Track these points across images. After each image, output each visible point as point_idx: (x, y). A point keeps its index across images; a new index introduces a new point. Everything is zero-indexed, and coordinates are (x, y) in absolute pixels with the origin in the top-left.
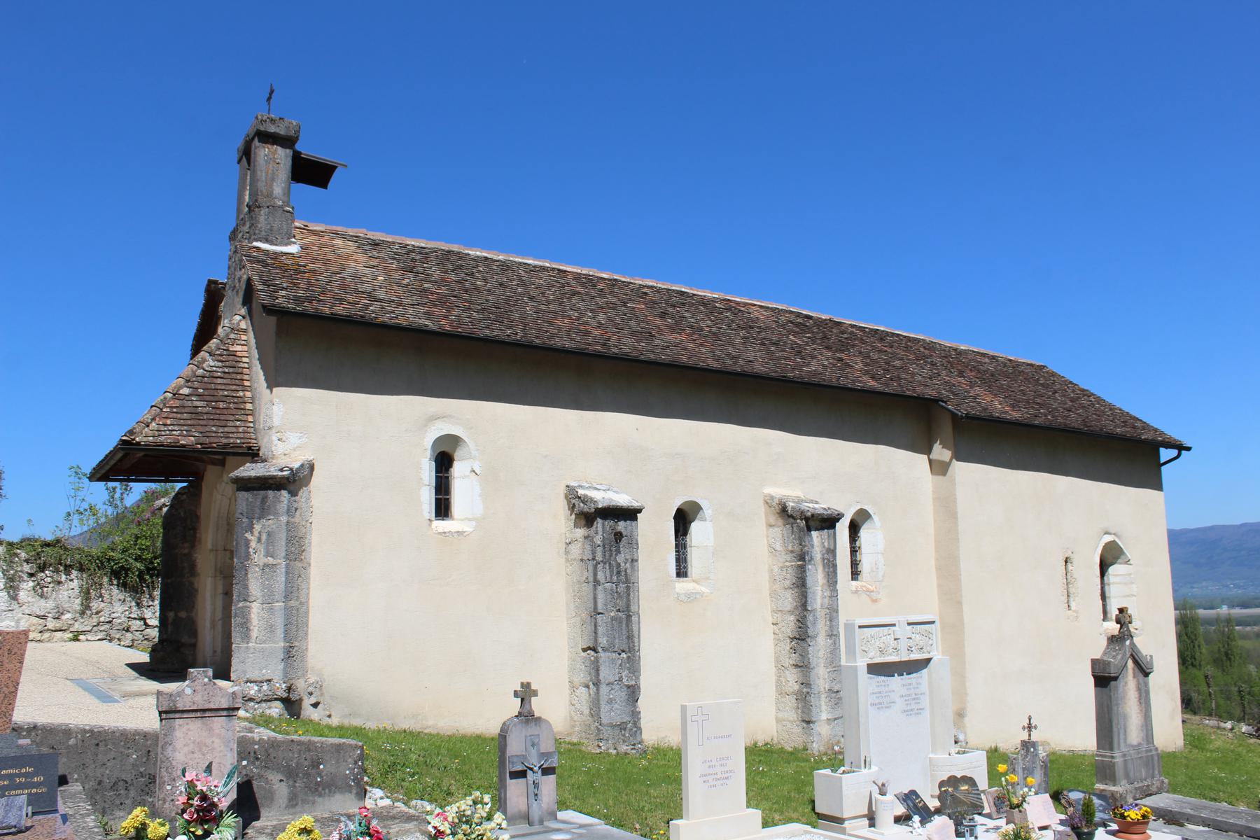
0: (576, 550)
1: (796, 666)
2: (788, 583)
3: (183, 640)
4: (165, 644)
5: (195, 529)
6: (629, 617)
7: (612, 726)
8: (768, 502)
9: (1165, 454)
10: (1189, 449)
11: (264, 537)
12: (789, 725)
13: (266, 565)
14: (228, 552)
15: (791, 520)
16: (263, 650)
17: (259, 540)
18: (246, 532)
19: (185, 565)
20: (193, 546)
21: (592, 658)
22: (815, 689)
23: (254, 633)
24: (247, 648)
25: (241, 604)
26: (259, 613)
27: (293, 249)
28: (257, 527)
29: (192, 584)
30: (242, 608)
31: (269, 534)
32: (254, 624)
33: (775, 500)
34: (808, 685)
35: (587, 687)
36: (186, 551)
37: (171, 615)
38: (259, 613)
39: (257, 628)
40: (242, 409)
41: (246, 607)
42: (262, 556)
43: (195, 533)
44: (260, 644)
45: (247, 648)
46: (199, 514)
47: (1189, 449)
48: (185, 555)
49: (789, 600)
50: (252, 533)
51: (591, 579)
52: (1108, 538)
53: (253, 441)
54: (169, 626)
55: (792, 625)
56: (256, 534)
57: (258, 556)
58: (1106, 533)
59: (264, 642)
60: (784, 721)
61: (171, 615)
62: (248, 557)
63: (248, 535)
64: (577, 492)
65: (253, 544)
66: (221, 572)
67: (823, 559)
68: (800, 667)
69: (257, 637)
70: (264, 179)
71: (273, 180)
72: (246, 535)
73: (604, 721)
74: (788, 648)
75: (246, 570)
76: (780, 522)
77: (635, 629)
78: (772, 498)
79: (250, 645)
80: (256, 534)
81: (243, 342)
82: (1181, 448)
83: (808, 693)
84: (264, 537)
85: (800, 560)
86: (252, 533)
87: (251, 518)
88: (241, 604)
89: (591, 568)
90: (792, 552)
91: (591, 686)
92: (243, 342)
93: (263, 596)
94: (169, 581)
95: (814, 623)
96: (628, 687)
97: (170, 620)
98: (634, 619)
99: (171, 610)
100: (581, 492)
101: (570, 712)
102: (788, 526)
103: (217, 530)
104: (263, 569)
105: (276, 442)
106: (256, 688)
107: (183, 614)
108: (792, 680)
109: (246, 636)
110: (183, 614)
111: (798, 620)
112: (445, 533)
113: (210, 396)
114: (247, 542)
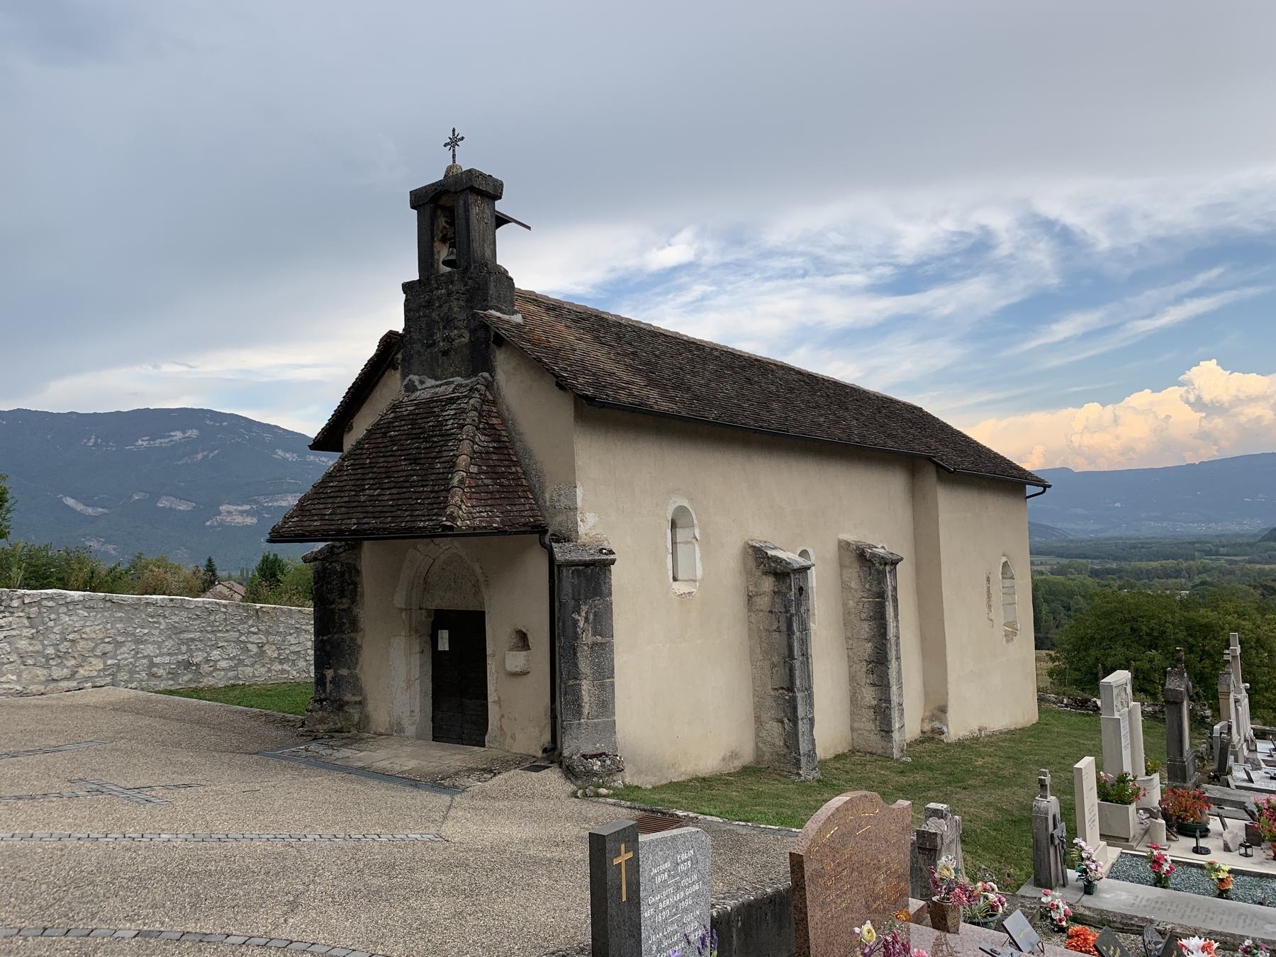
0: (763, 602)
1: (873, 685)
2: (864, 616)
3: (346, 698)
4: (324, 703)
5: (355, 584)
6: (808, 658)
7: (805, 755)
8: (844, 546)
9: (1030, 490)
10: (1050, 486)
11: (591, 617)
12: (866, 733)
13: (595, 644)
14: (423, 611)
15: (870, 563)
16: (596, 725)
17: (587, 620)
18: (573, 612)
19: (345, 621)
20: (353, 601)
21: (787, 698)
22: (892, 706)
23: (586, 711)
24: (579, 724)
25: (571, 683)
26: (590, 690)
27: (518, 318)
28: (584, 608)
29: (353, 640)
30: (572, 686)
31: (595, 615)
32: (585, 701)
33: (851, 546)
34: (888, 701)
35: (782, 722)
36: (345, 606)
37: (329, 674)
38: (590, 690)
39: (588, 704)
40: (520, 485)
41: (576, 684)
42: (590, 634)
43: (356, 587)
44: (592, 719)
45: (579, 724)
46: (359, 569)
47: (1050, 486)
48: (343, 610)
49: (866, 628)
50: (579, 614)
51: (784, 628)
52: (1004, 559)
53: (540, 518)
54: (328, 684)
55: (869, 651)
56: (583, 614)
57: (587, 635)
58: (1004, 555)
59: (597, 717)
60: (861, 730)
61: (329, 674)
62: (576, 636)
63: (577, 617)
64: (767, 554)
65: (581, 624)
66: (417, 631)
67: (892, 596)
68: (878, 686)
69: (589, 713)
70: (477, 240)
71: (484, 241)
72: (573, 616)
73: (802, 752)
74: (864, 669)
75: (574, 649)
76: (856, 565)
77: (811, 668)
78: (848, 544)
79: (582, 721)
80: (583, 614)
81: (496, 414)
82: (1046, 487)
83: (888, 707)
84: (591, 617)
85: (877, 598)
86: (579, 614)
87: (577, 600)
88: (571, 683)
89: (783, 620)
90: (868, 590)
91: (786, 720)
92: (496, 414)
93: (593, 673)
94: (325, 638)
95: (890, 650)
96: (810, 719)
97: (329, 678)
98: (810, 660)
99: (330, 668)
100: (770, 553)
101: (756, 743)
102: (865, 569)
103: (412, 588)
104: (592, 648)
105: (580, 523)
106: (599, 763)
107: (344, 672)
108: (869, 696)
109: (578, 713)
110: (344, 672)
111: (876, 647)
112: (681, 595)
113: (494, 474)
114: (575, 622)
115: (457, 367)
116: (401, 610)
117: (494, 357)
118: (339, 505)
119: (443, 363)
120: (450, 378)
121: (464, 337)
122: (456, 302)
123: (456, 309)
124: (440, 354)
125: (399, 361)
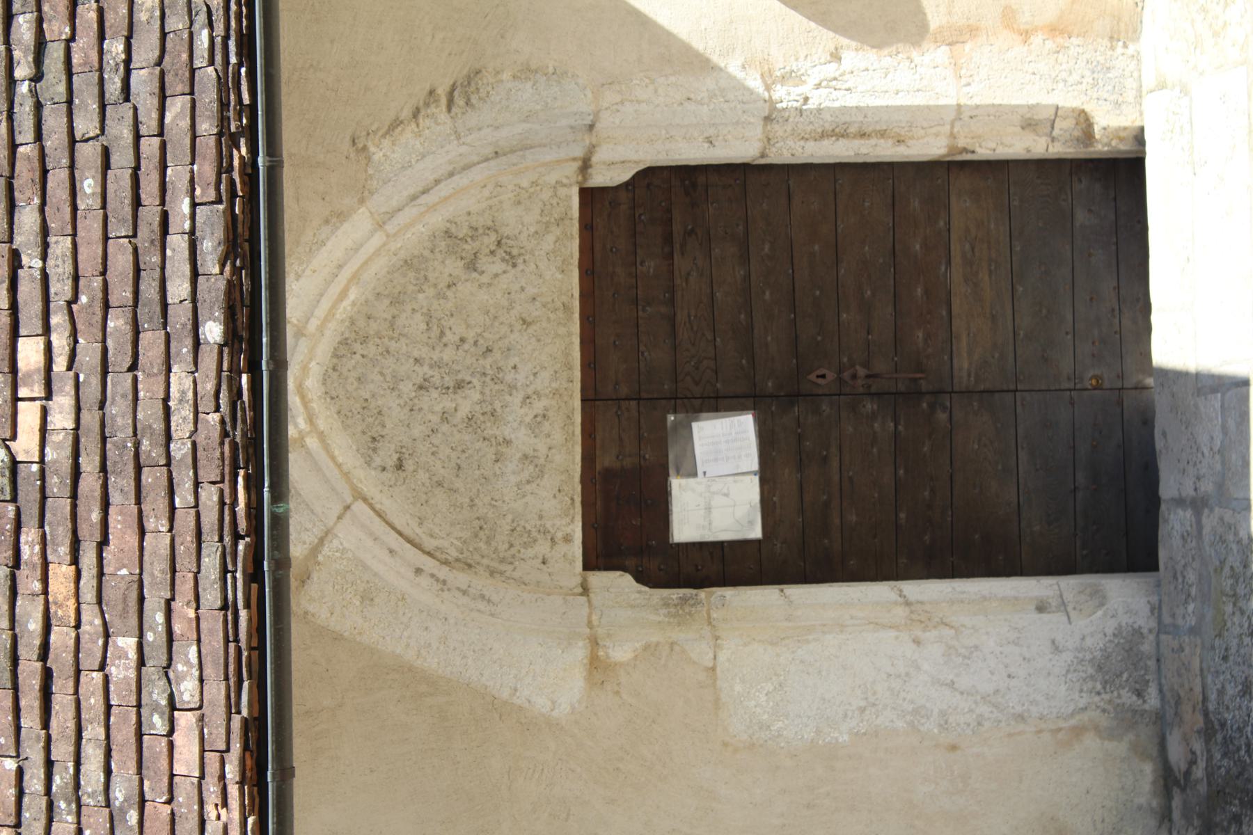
116: (597, 666)
118: (88, 594)
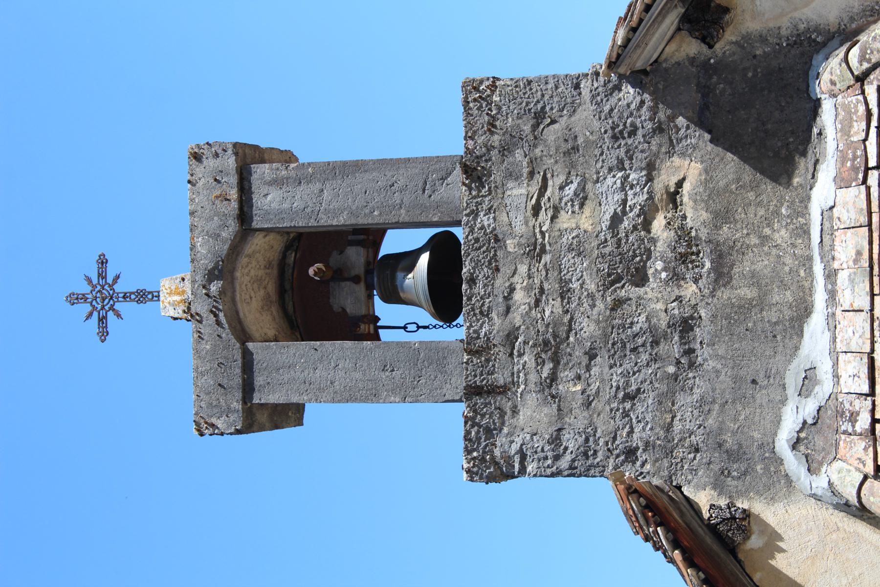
115: (777, 213)
117: (763, 39)
119: (755, 279)
120: (809, 246)
121: (680, 184)
122: (565, 221)
123: (585, 222)
124: (724, 294)
125: (723, 502)
